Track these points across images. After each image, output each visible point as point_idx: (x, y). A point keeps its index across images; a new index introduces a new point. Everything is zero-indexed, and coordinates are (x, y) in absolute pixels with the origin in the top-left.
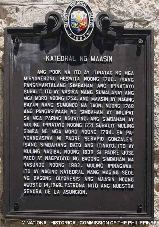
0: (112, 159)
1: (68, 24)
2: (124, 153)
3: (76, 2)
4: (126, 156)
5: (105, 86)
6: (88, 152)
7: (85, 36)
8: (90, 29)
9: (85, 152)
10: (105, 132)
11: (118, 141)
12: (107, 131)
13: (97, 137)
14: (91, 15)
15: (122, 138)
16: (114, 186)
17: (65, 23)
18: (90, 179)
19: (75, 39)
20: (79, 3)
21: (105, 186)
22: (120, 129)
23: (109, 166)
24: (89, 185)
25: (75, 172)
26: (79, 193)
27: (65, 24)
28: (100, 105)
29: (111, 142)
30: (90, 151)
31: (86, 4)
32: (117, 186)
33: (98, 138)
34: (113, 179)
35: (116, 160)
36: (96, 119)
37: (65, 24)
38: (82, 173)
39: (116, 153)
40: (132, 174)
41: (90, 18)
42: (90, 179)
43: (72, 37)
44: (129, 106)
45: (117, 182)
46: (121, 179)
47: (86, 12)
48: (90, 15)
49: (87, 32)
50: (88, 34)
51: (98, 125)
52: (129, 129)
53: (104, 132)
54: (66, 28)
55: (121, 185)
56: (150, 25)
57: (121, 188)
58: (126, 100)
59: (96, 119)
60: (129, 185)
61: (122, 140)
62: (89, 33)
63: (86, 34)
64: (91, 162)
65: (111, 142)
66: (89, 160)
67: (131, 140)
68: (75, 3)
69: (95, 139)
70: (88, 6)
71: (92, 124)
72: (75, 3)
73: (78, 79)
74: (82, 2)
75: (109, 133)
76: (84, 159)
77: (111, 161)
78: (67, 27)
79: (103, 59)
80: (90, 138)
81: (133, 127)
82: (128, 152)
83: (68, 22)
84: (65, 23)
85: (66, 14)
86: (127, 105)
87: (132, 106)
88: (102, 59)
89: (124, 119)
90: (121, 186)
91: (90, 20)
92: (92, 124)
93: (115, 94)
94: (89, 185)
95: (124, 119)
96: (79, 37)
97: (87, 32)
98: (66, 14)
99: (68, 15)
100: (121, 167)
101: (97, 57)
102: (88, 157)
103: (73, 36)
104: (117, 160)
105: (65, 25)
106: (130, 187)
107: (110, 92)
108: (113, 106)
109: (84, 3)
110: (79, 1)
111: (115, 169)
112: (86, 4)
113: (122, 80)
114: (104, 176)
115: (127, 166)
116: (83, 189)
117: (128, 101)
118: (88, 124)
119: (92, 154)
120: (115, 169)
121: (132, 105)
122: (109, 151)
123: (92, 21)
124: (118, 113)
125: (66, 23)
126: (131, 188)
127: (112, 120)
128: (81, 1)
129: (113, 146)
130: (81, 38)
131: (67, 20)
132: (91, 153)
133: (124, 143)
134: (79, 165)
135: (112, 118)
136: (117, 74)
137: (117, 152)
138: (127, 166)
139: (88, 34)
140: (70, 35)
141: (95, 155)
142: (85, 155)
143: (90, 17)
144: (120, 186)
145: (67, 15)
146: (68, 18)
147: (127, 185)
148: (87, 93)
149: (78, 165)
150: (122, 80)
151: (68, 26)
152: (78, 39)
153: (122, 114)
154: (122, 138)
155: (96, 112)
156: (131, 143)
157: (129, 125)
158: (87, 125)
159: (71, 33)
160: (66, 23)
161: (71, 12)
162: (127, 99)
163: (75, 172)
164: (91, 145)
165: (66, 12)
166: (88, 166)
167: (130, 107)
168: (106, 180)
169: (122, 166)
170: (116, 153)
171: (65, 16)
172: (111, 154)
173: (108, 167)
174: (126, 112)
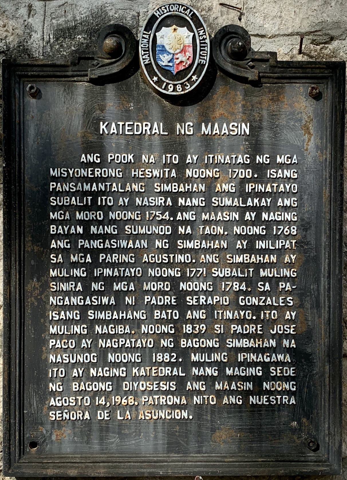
0: (247, 343)
1: (149, 56)
2: (273, 331)
3: (167, 7)
4: (279, 337)
5: (233, 188)
6: (194, 328)
7: (187, 84)
8: (201, 66)
9: (188, 329)
10: (232, 286)
11: (261, 304)
12: (236, 285)
13: (215, 297)
14: (202, 35)
15: (269, 299)
16: (253, 400)
17: (143, 53)
18: (198, 386)
19: (166, 88)
20: (175, 9)
21: (233, 400)
22: (265, 279)
23: (241, 357)
24: (197, 400)
25: (166, 371)
26: (173, 417)
27: (142, 56)
28: (220, 230)
29: (245, 308)
30: (198, 327)
31: (191, 11)
32: (260, 401)
33: (216, 299)
34: (249, 386)
35: (257, 346)
36: (210, 258)
37: (142, 56)
38: (181, 374)
39: (256, 330)
40: (291, 375)
41: (201, 43)
42: (198, 386)
43: (159, 86)
44: (286, 229)
45: (259, 391)
46: (266, 386)
47: (191, 30)
48: (199, 36)
49: (193, 74)
50: (194, 78)
51: (218, 271)
52: (285, 279)
53: (230, 286)
54: (145, 65)
55: (268, 398)
56: (335, 44)
57: (268, 403)
58: (280, 217)
59: (210, 258)
60: (285, 398)
61: (269, 302)
62: (198, 77)
63: (191, 77)
64: (201, 350)
65: (245, 308)
66: (196, 344)
67: (290, 303)
68: (166, 8)
69: (210, 301)
70: (194, 17)
71: (203, 270)
72: (166, 8)
73: (173, 174)
74: (183, 6)
75: (241, 288)
76: (183, 343)
77: (245, 346)
78: (147, 63)
79: (229, 130)
80: (199, 298)
81: (294, 275)
82: (282, 329)
83: (148, 51)
84: (143, 53)
85: (144, 34)
86: (282, 227)
87: (292, 230)
88: (226, 129)
89: (273, 258)
90: (269, 400)
91: (201, 47)
92: (203, 270)
93: (255, 205)
94: (197, 400)
95: (273, 258)
96: (175, 85)
97: (193, 74)
98: (144, 34)
99: (150, 35)
100: (268, 360)
101: (216, 125)
102: (194, 340)
103: (159, 82)
104: (259, 345)
105: (143, 59)
106: (289, 401)
107: (245, 202)
108: (250, 232)
109: (188, 8)
110: (174, 4)
111: (254, 364)
112: (191, 11)
113: (270, 174)
114: (231, 379)
115: (280, 357)
116: (181, 407)
117: (283, 219)
118: (195, 270)
119: (203, 332)
120: (254, 364)
121: (294, 228)
122: (240, 326)
123: (204, 50)
124: (260, 245)
125: (145, 54)
126: (290, 403)
127: (247, 260)
128: (179, 5)
129: (249, 315)
130: (179, 87)
131: (148, 47)
132: (200, 331)
133: (276, 308)
134: (173, 356)
135: (247, 257)
136: (266, 388)
137: (259, 329)
138: (280, 357)
139: (194, 78)
140: (153, 81)
141: (209, 335)
142: (187, 336)
143: (200, 40)
144: (265, 400)
145: (147, 37)
146: (149, 41)
147: (281, 398)
148: (191, 203)
149: (171, 357)
150: (270, 174)
151: (150, 60)
152: (172, 89)
153: (271, 248)
154: (269, 299)
155: (212, 245)
156: (290, 308)
157: (285, 269)
158: (191, 272)
159: (157, 75)
160: (145, 54)
161: (158, 29)
162: (281, 215)
163: (166, 371)
164: (200, 314)
165: (145, 30)
166: (194, 358)
167: (289, 232)
168: (234, 387)
169: (270, 356)
170: (256, 330)
171: (143, 38)
172: (245, 332)
173: (239, 361)
174: (279, 244)
